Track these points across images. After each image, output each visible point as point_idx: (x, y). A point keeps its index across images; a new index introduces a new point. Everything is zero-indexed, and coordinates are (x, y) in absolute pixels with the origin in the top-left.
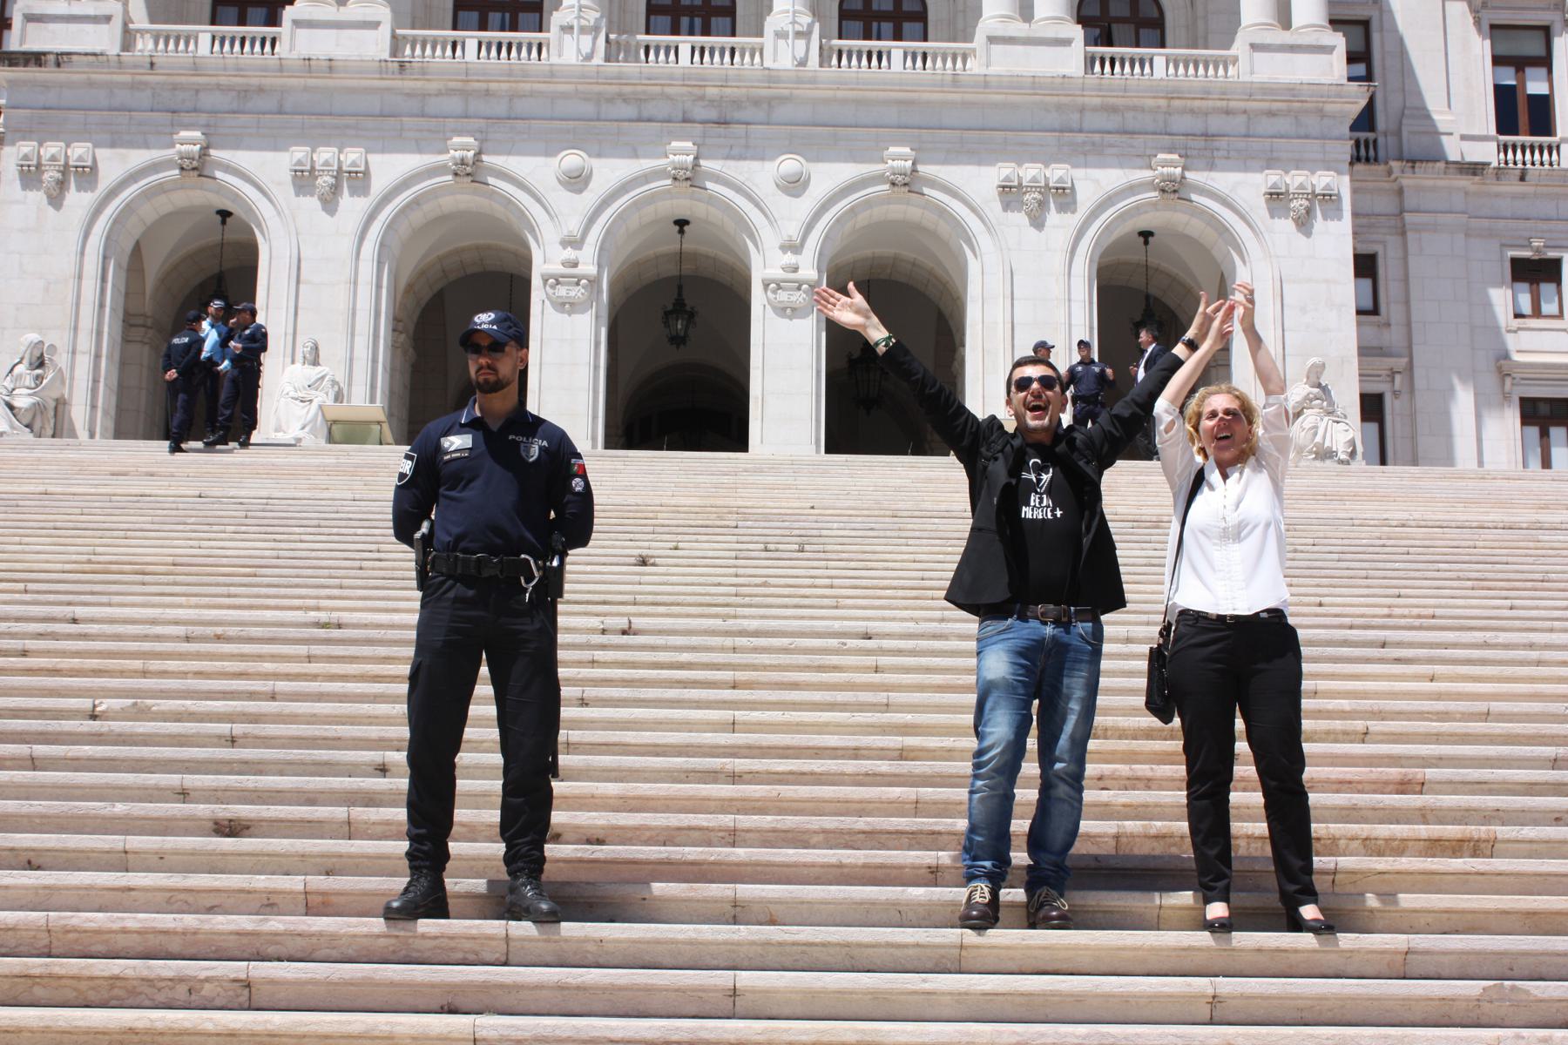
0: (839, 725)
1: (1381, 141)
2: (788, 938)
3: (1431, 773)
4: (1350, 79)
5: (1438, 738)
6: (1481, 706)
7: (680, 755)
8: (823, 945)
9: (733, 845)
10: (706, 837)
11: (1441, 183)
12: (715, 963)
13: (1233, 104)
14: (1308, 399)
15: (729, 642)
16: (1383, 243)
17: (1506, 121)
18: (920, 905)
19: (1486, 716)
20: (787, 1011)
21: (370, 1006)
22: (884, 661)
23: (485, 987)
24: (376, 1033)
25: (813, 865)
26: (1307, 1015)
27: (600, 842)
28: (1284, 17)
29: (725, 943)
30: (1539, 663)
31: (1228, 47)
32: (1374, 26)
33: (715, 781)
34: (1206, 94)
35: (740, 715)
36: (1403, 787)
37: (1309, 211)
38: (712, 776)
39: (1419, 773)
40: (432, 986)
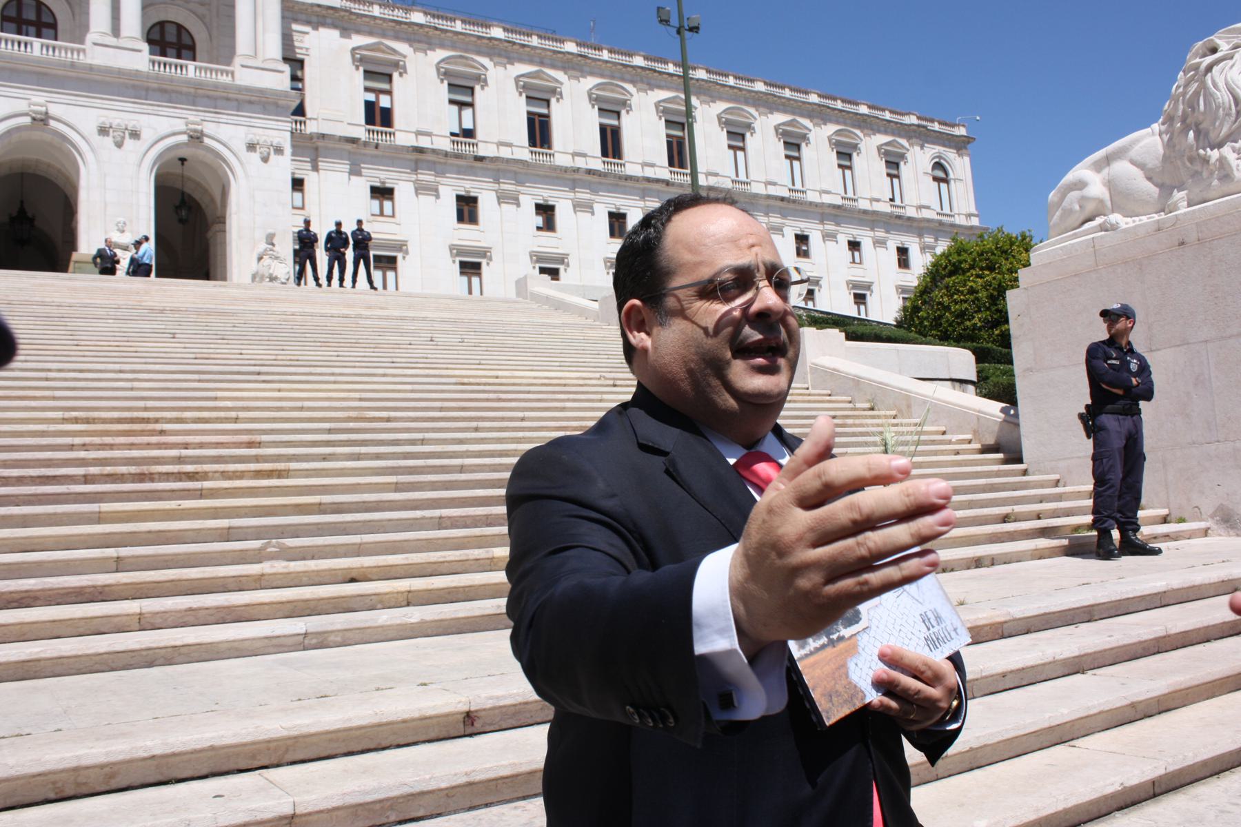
3: (265, 438)
5: (274, 420)
6: (299, 404)
17: (370, 120)
19: (301, 409)
30: (335, 382)
36: (250, 445)
39: (258, 438)
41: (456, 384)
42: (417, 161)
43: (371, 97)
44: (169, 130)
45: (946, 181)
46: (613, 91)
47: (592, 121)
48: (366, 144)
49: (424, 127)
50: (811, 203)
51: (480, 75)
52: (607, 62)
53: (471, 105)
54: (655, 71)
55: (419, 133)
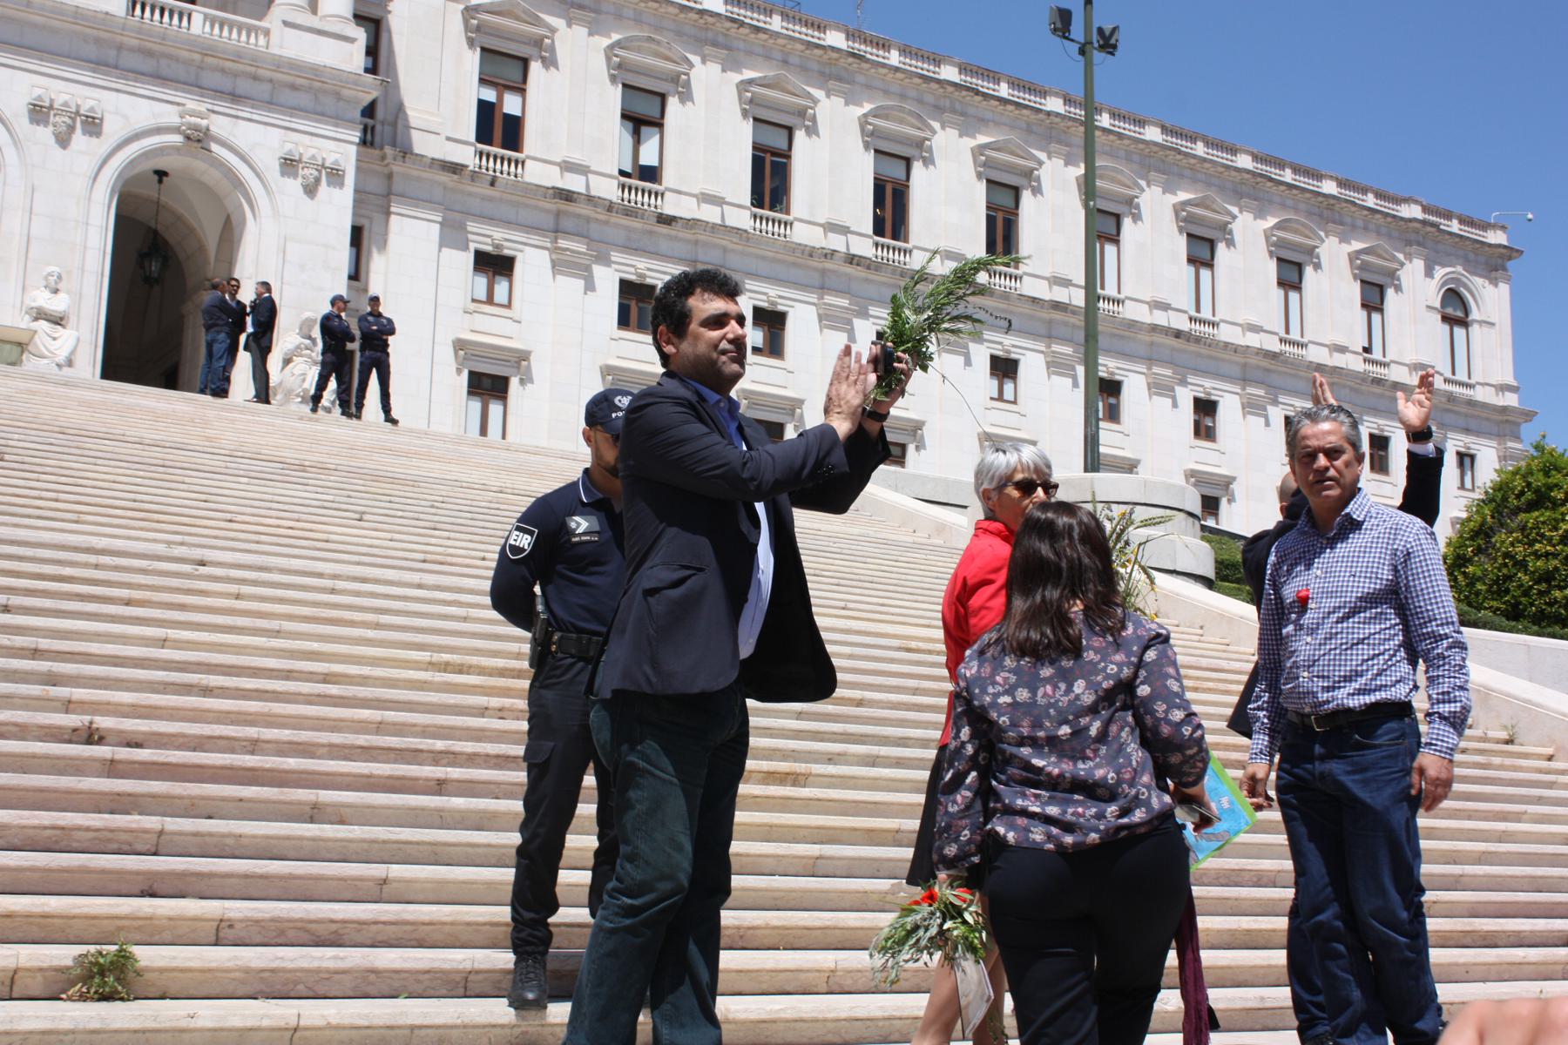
0: (256, 648)
1: (378, 128)
2: (393, 837)
4: (367, 70)
7: (136, 666)
8: (418, 843)
9: (252, 753)
10: (230, 744)
11: (424, 175)
12: (328, 856)
13: (261, 72)
14: (298, 347)
15: (93, 559)
16: (370, 219)
17: (484, 135)
18: (459, 811)
20: (421, 897)
21: (82, 890)
22: (246, 589)
23: (183, 875)
24: (140, 914)
25: (348, 775)
26: (780, 903)
27: (138, 745)
28: (313, 5)
29: (341, 840)
31: (260, 19)
32: (383, 27)
33: (188, 694)
34: (238, 56)
35: (172, 633)
37: (318, 180)
38: (187, 689)
40: (138, 873)
41: (899, 649)
42: (558, 214)
43: (490, 95)
44: (149, 122)
45: (1464, 323)
46: (901, 121)
47: (862, 171)
48: (475, 176)
49: (576, 157)
50: (1226, 344)
51: (679, 75)
52: (897, 69)
53: (658, 124)
54: (977, 93)
55: (568, 167)
